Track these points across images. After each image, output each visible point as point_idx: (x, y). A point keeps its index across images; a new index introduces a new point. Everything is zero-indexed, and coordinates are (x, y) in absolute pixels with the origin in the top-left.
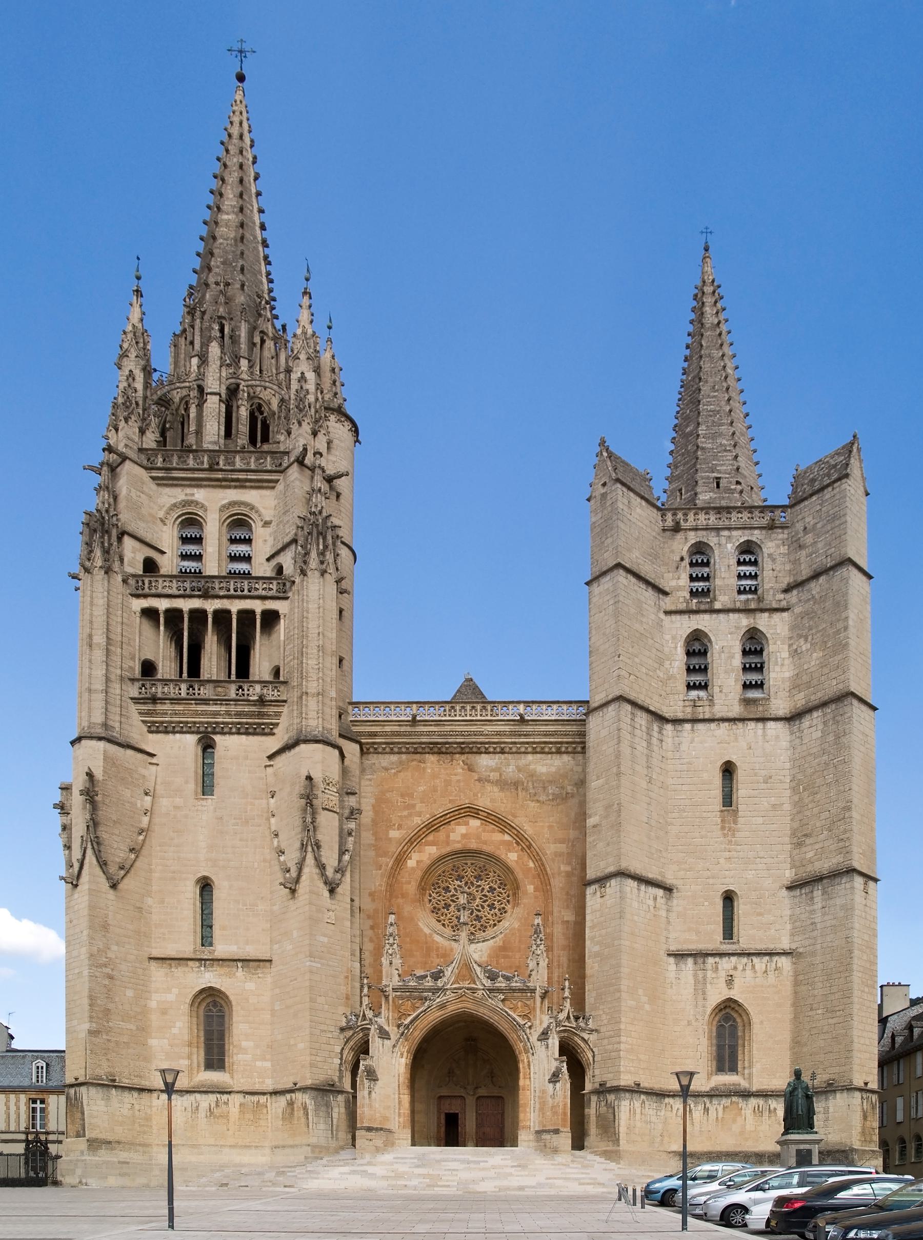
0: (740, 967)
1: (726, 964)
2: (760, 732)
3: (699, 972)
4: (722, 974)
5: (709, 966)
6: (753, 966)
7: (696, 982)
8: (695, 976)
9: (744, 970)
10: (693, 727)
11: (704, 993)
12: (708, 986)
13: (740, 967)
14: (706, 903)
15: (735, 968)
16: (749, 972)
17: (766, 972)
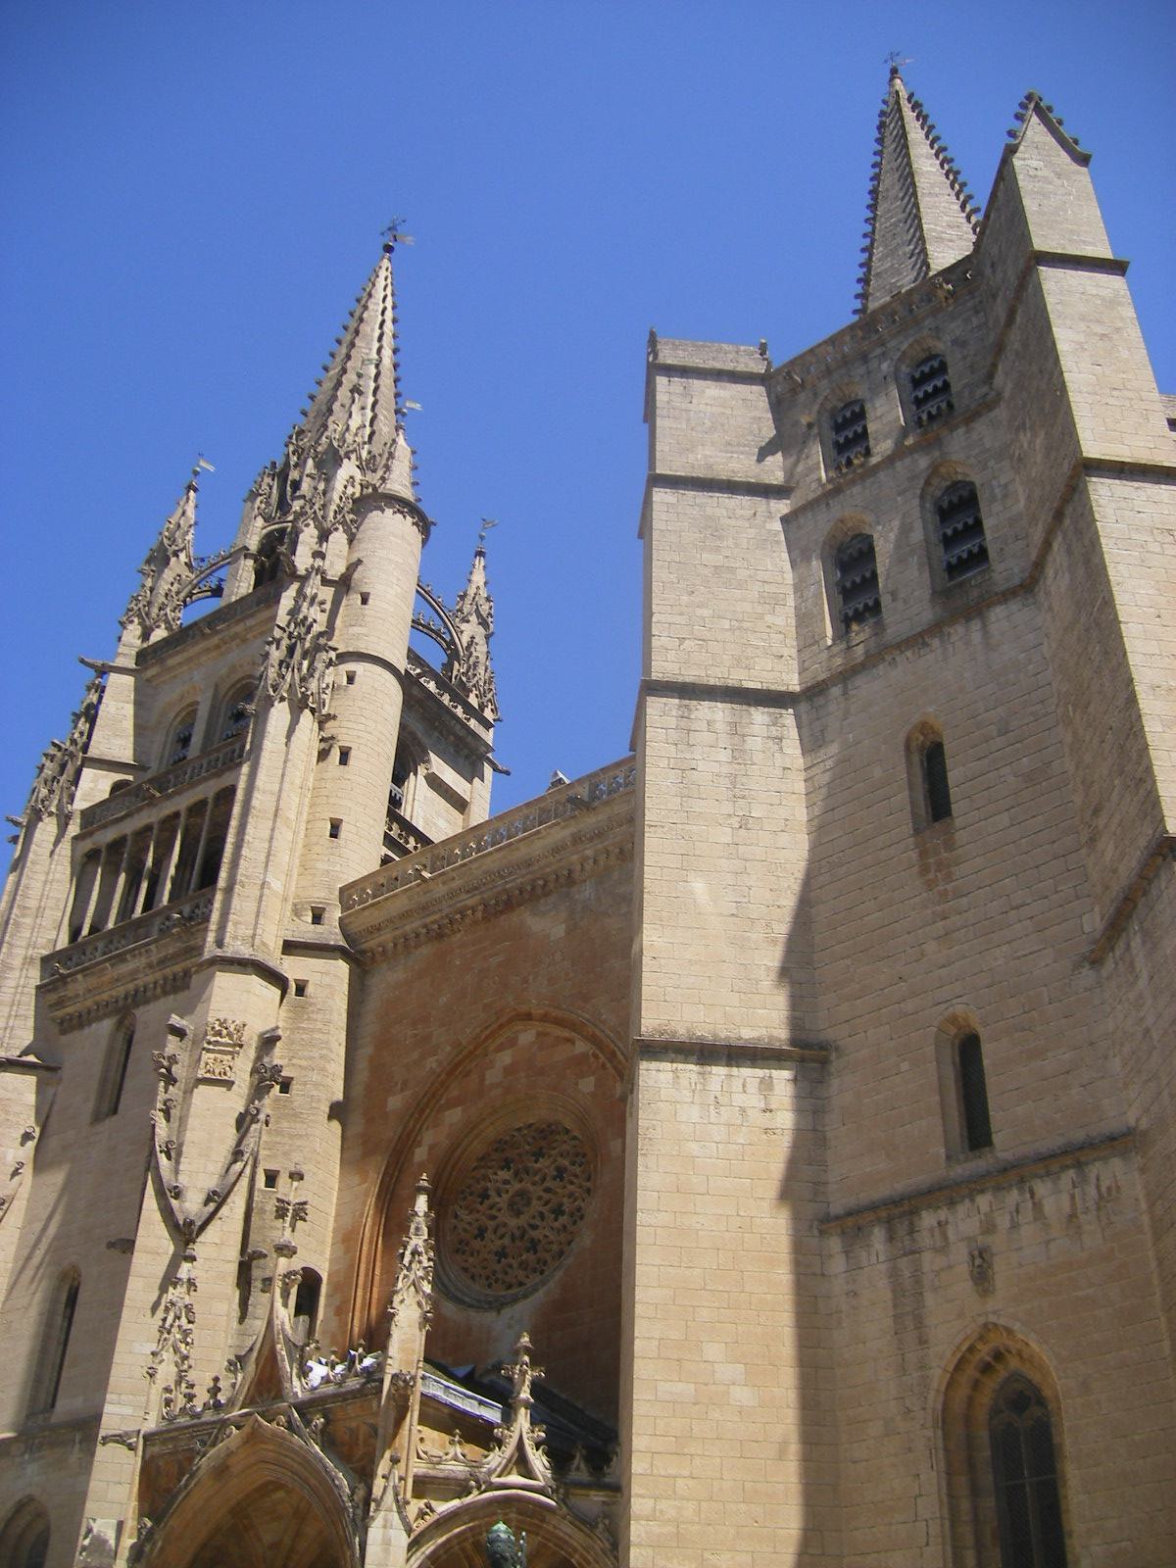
0: (1003, 1221)
1: (964, 1221)
2: (976, 637)
3: (904, 1263)
4: (960, 1254)
5: (925, 1239)
6: (1037, 1207)
7: (897, 1290)
8: (894, 1274)
9: (1015, 1226)
10: (845, 688)
11: (919, 1322)
12: (930, 1299)
13: (1003, 1221)
14: (905, 1066)
15: (989, 1228)
16: (1028, 1231)
17: (1072, 1216)
